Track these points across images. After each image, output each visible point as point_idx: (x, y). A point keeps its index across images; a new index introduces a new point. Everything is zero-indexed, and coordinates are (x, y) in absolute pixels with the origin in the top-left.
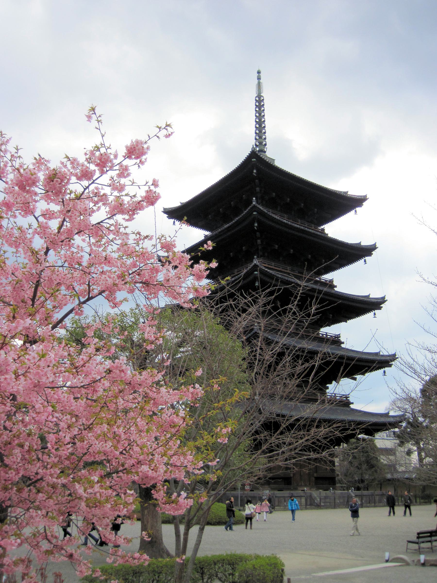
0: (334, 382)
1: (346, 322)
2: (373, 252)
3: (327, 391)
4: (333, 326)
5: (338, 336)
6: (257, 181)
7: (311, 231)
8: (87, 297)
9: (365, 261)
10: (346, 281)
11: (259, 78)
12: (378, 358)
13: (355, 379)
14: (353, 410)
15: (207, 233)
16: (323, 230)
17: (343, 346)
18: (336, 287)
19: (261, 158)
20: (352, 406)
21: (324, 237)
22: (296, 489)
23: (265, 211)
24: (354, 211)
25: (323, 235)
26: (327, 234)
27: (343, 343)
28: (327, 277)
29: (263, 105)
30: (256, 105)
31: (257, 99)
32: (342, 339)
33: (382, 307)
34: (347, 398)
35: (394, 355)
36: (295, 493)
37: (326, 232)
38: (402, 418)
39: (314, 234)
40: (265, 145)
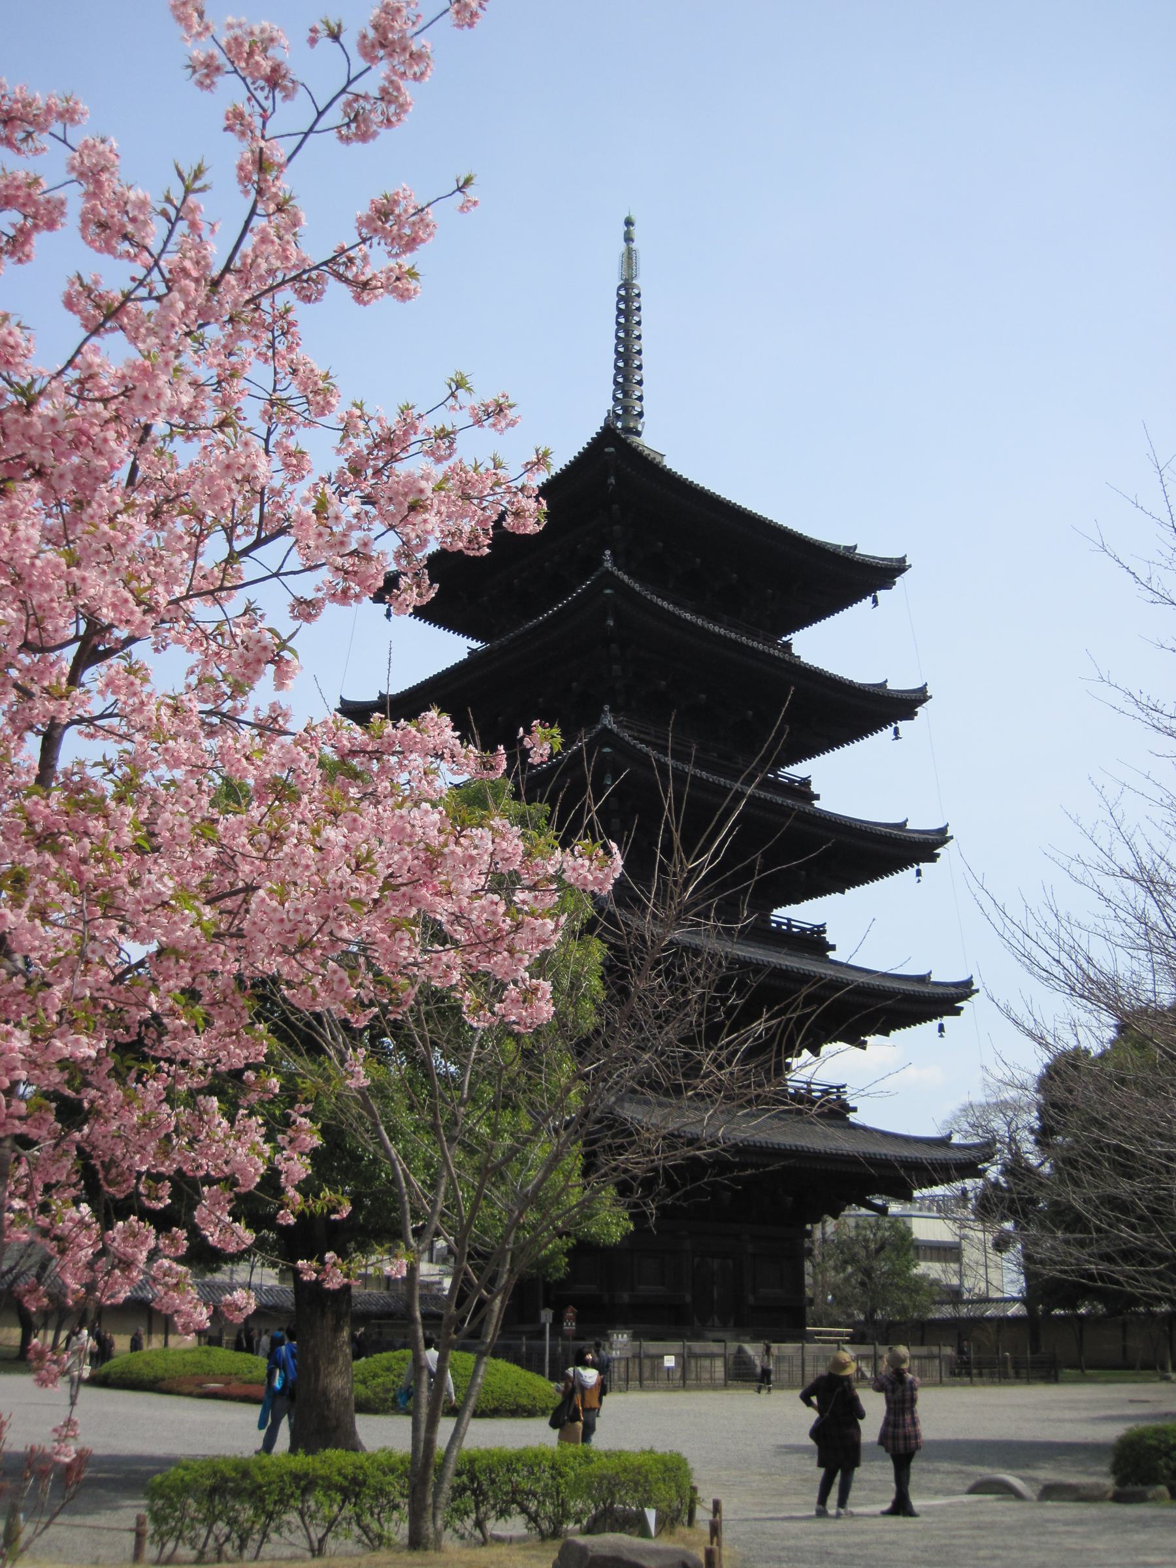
0: (805, 1052)
4: (807, 905)
5: (820, 930)
7: (755, 644)
8: (253, 538)
9: (896, 731)
10: (846, 782)
11: (628, 238)
13: (863, 1045)
14: (854, 1127)
15: (476, 645)
16: (787, 646)
17: (831, 955)
18: (817, 797)
19: (629, 445)
20: (852, 1117)
22: (698, 1337)
23: (637, 587)
24: (870, 599)
25: (787, 657)
27: (833, 948)
29: (639, 309)
30: (619, 309)
31: (623, 293)
32: (830, 937)
33: (938, 855)
35: (968, 983)
36: (697, 1347)
37: (795, 650)
38: (986, 1150)
39: (763, 652)
40: (641, 415)
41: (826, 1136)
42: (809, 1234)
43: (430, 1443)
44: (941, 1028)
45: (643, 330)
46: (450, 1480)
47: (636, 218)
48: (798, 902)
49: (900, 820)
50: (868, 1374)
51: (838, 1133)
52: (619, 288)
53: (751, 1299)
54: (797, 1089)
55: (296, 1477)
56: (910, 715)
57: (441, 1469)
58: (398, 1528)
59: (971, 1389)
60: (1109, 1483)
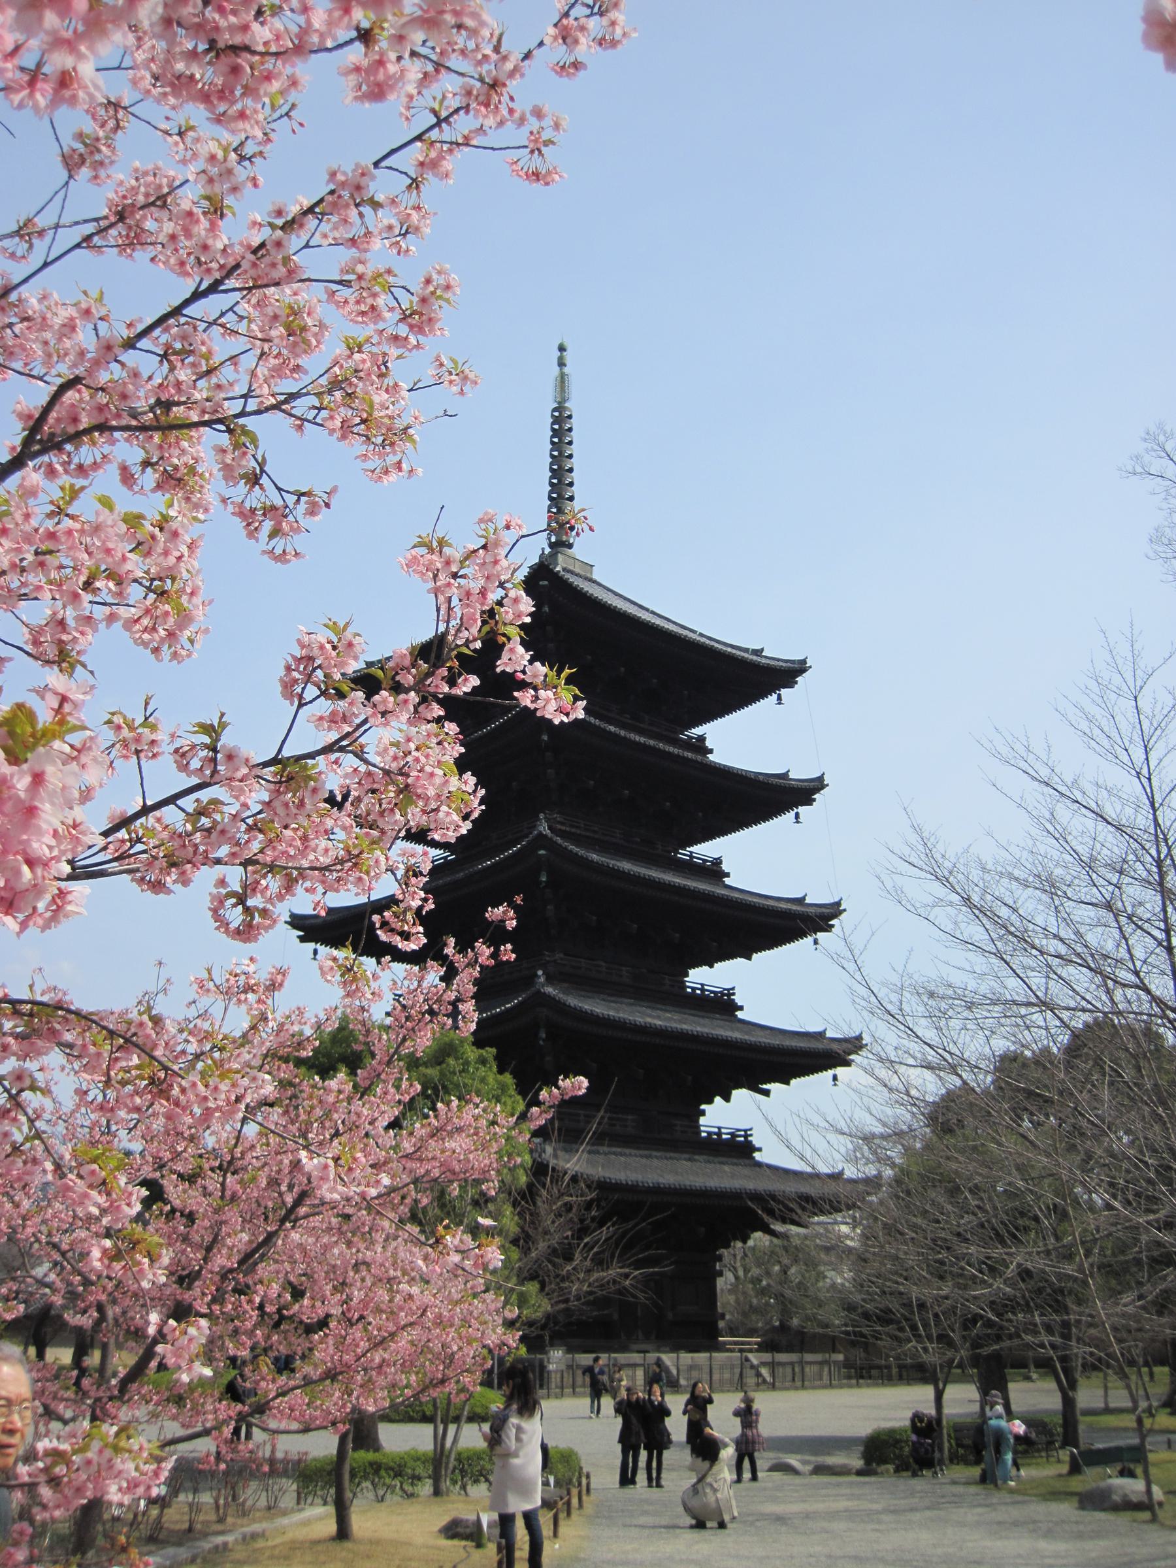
0: (718, 1099)
1: (749, 959)
3: (702, 1121)
4: (718, 966)
5: (730, 992)
6: (549, 628)
7: (671, 749)
9: (797, 816)
10: (752, 860)
11: (561, 364)
13: (766, 1093)
14: (759, 1165)
16: (702, 739)
17: (739, 1014)
21: (701, 763)
22: (624, 1349)
24: (775, 696)
25: (699, 758)
26: (711, 751)
27: (741, 1008)
28: (705, 850)
29: (570, 430)
30: (553, 430)
32: (738, 999)
34: (746, 1136)
35: (859, 1038)
36: (622, 1357)
37: (709, 744)
38: (872, 1183)
42: (720, 1258)
43: (443, 1445)
44: (835, 1078)
45: (574, 449)
46: (452, 1462)
48: (711, 966)
50: (769, 1379)
51: (746, 1171)
52: (555, 410)
53: (670, 1316)
54: (709, 1133)
55: (371, 1464)
56: (809, 801)
57: (448, 1457)
58: (426, 1488)
59: (856, 1392)
60: (858, 1463)
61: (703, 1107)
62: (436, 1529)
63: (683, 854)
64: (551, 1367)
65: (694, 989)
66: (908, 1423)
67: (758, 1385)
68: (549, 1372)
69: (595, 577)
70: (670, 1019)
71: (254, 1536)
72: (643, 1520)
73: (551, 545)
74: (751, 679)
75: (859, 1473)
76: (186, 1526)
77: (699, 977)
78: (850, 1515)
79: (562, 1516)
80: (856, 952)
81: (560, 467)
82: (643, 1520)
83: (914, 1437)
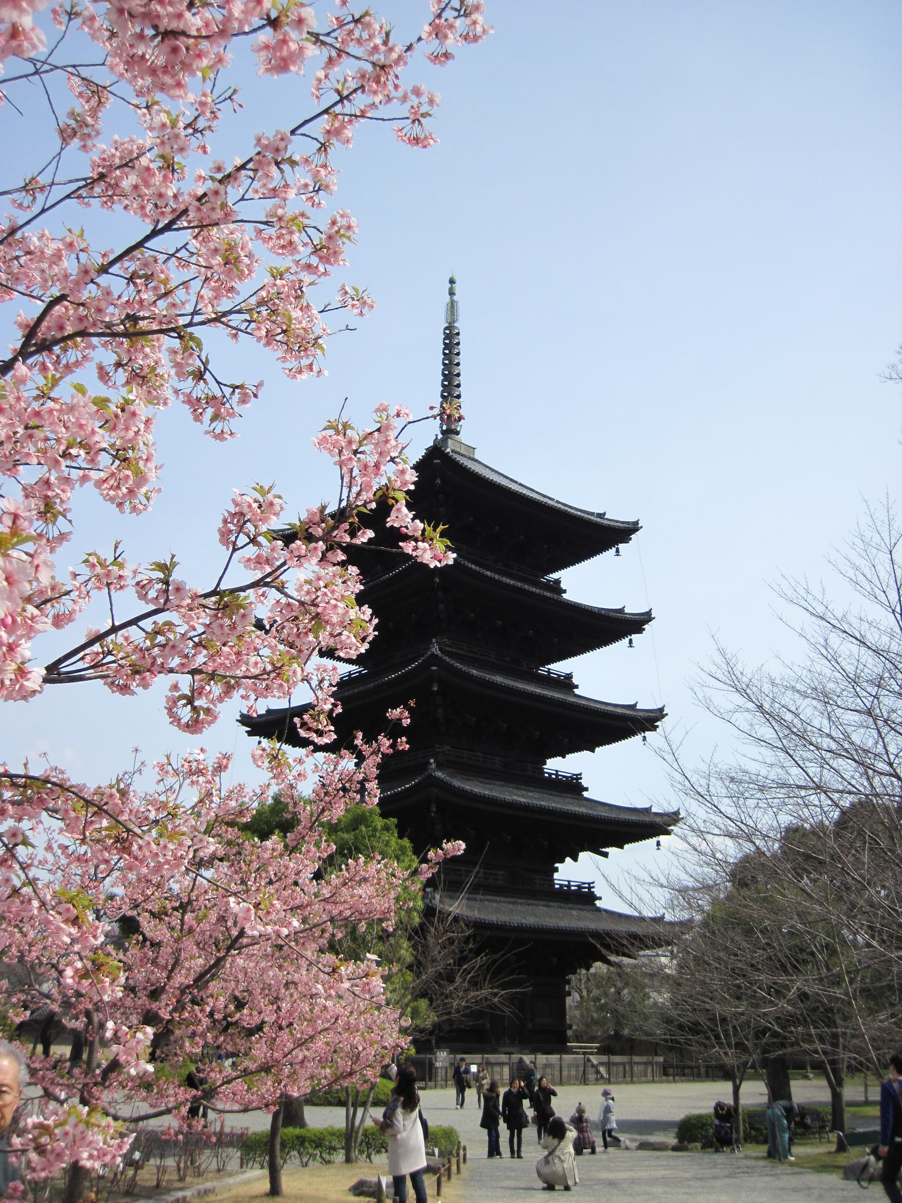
0: (568, 859)
2: (646, 627)
3: (556, 876)
5: (578, 777)
6: (441, 496)
9: (631, 641)
10: (596, 676)
11: (452, 293)
12: (647, 819)
13: (605, 855)
14: (599, 910)
16: (558, 582)
17: (585, 794)
22: (494, 1051)
24: (614, 549)
25: (555, 596)
26: (565, 592)
27: (586, 789)
28: (560, 667)
29: (458, 344)
30: (445, 344)
32: (584, 782)
34: (590, 888)
35: (677, 813)
36: (492, 1057)
38: (686, 925)
41: (579, 919)
42: (569, 982)
43: (353, 1123)
44: (658, 844)
45: (461, 359)
46: (360, 1137)
47: (457, 279)
48: (564, 757)
49: (631, 702)
51: (589, 915)
52: (446, 329)
53: (530, 1026)
55: (298, 1137)
56: (640, 630)
57: (357, 1133)
58: (340, 1156)
59: (673, 1085)
61: (557, 865)
62: (347, 1188)
63: (543, 670)
64: (438, 1064)
65: (550, 774)
66: (712, 1111)
67: (597, 1080)
68: (436, 1068)
69: (476, 457)
70: (532, 798)
71: (207, 1192)
72: (507, 1183)
73: (443, 432)
74: (597, 536)
75: (674, 1149)
76: (155, 1183)
77: (554, 765)
78: (665, 1181)
79: (444, 1179)
80: (674, 747)
81: (450, 373)
82: (507, 1183)
83: (717, 1122)
